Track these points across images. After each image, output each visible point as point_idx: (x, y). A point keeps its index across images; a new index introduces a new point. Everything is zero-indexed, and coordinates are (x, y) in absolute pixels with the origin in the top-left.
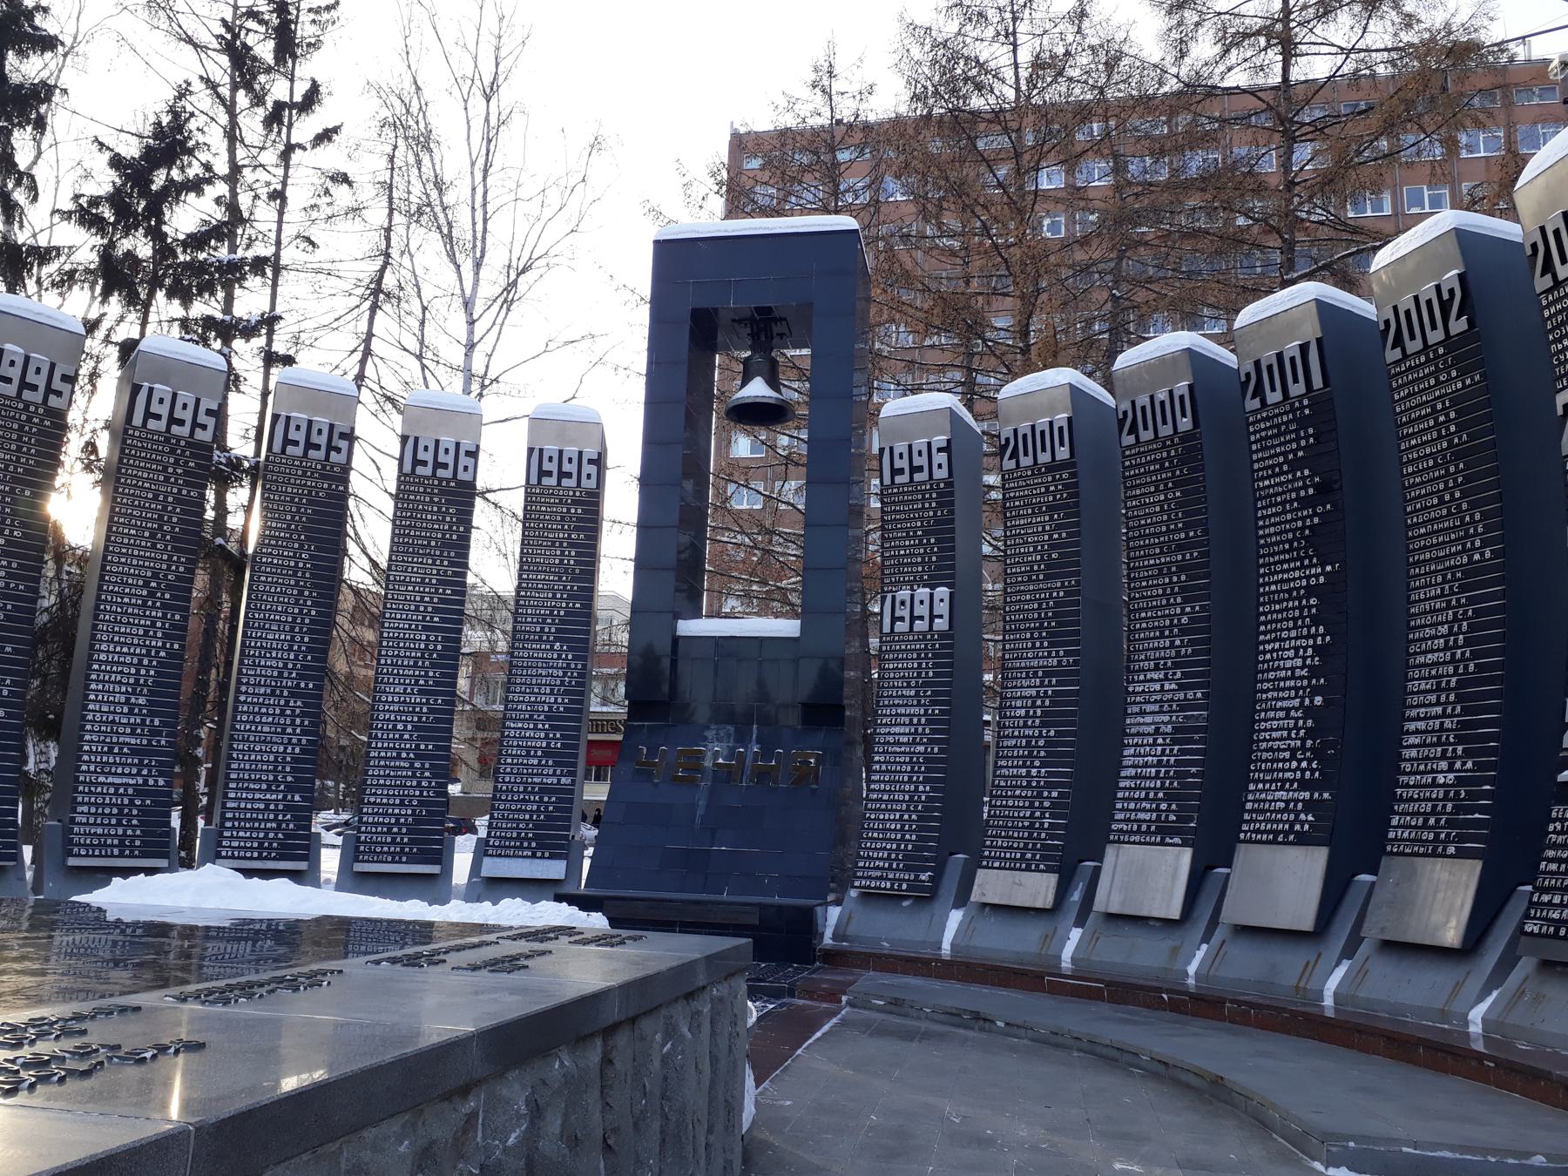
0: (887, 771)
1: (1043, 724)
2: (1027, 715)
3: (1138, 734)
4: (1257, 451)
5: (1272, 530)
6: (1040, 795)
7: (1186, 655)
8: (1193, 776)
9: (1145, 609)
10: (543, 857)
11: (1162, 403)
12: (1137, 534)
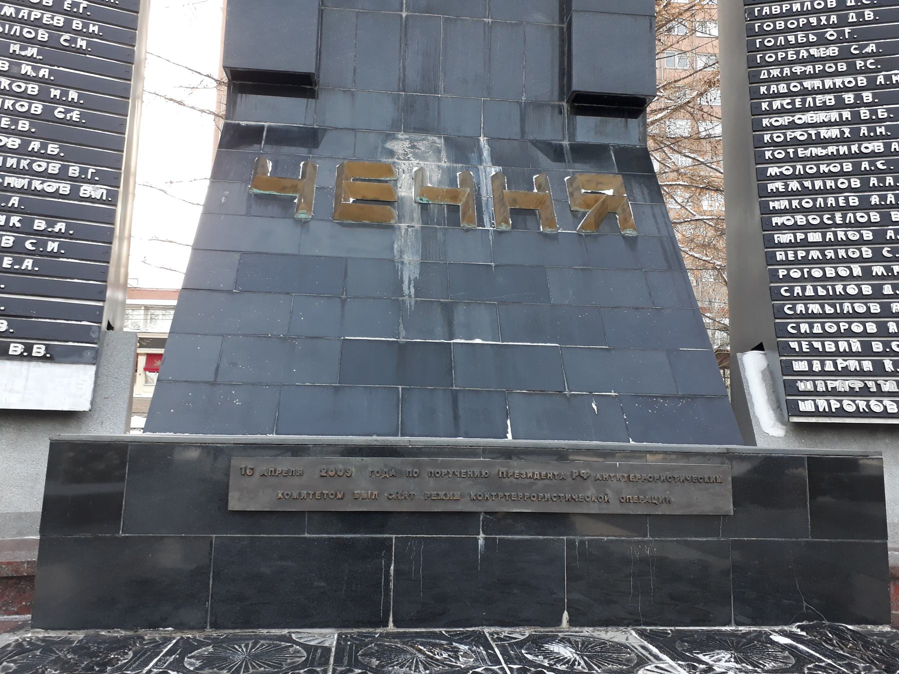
10: (27, 356)
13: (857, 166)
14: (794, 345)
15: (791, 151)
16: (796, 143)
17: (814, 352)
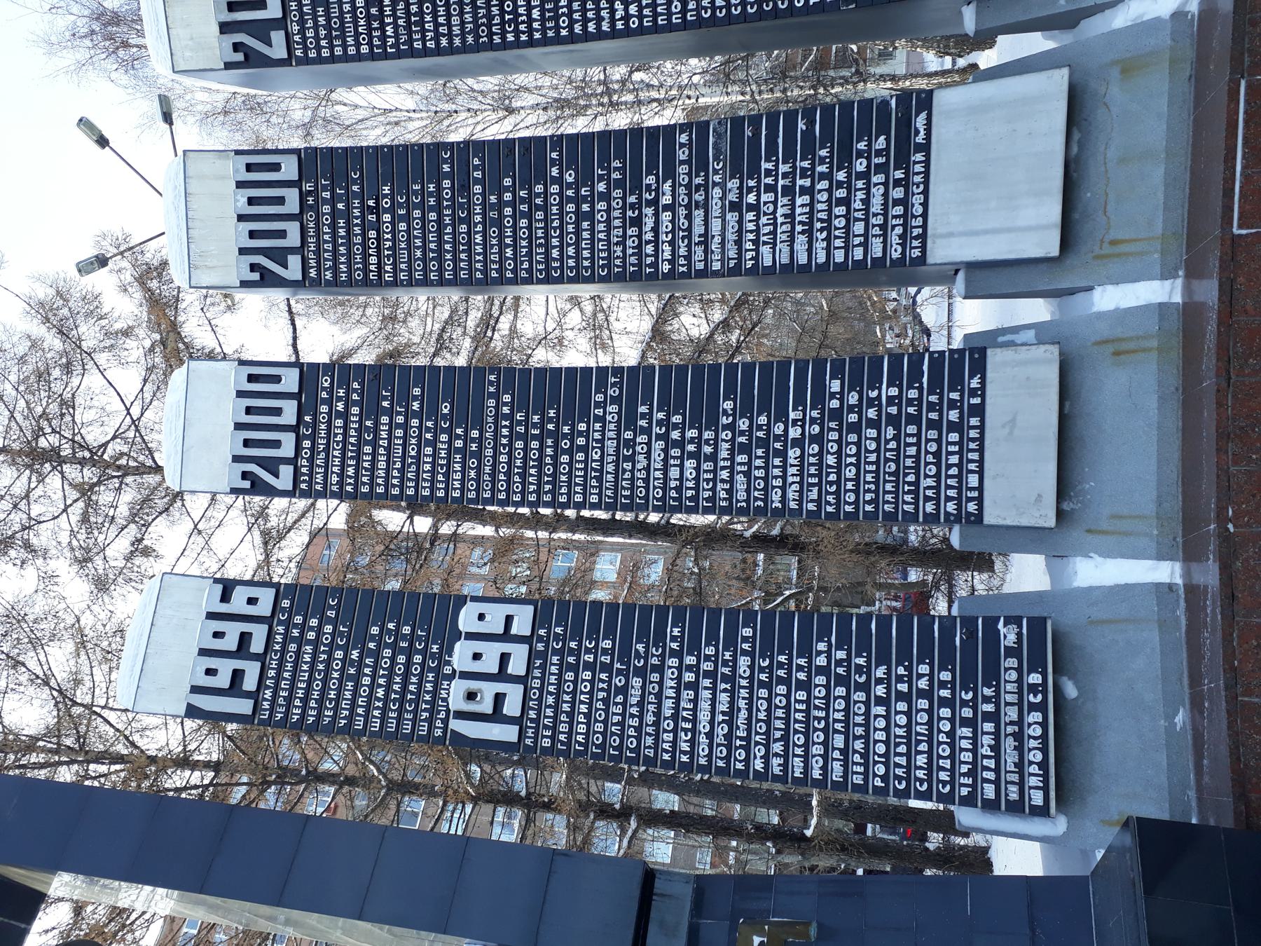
0: (785, 738)
1: (713, 423)
2: (696, 455)
3: (739, 243)
4: (345, 46)
5: (455, 20)
6: (837, 415)
7: (622, 170)
8: (810, 123)
9: (548, 247)
11: (251, 201)
12: (433, 265)
13: (762, 684)
14: (964, 791)
15: (738, 743)
16: (729, 737)
17: (972, 773)
